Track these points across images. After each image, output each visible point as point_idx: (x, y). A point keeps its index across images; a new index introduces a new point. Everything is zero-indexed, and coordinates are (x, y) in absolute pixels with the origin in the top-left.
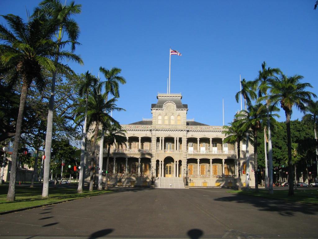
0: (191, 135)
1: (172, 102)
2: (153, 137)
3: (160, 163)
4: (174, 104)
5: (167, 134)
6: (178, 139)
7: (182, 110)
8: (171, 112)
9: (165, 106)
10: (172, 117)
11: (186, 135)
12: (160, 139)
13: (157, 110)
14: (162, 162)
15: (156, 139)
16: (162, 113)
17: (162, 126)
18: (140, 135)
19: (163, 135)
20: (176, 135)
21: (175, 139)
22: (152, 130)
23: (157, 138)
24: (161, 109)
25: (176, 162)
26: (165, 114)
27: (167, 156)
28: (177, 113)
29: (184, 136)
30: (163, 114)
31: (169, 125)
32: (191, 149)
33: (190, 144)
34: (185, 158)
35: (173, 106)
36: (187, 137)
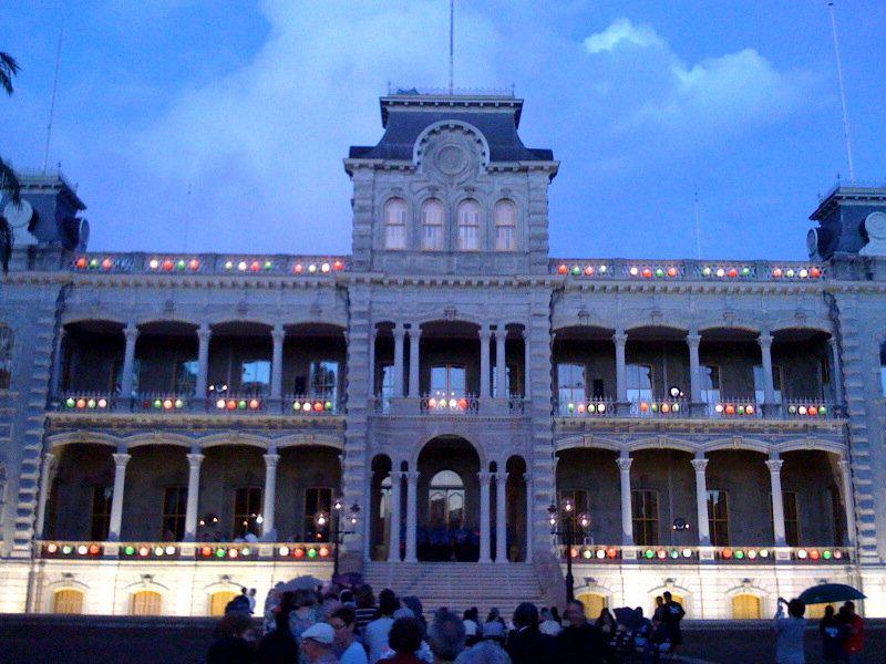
0: (576, 312)
1: (467, 126)
2: (355, 322)
3: (396, 472)
4: (479, 135)
5: (438, 305)
6: (502, 333)
7: (525, 170)
8: (456, 180)
9: (429, 148)
10: (468, 213)
11: (547, 311)
12: (399, 331)
13: (377, 168)
15: (375, 331)
16: (410, 186)
18: (279, 313)
19: (413, 310)
20: (487, 311)
21: (485, 333)
22: (348, 282)
23: (377, 325)
24: (402, 164)
25: (493, 467)
26: (425, 193)
27: (435, 434)
28: (498, 188)
29: (535, 315)
30: (415, 194)
31: (451, 253)
32: (576, 404)
33: (573, 373)
34: (544, 442)
35: (473, 152)
36: (555, 328)
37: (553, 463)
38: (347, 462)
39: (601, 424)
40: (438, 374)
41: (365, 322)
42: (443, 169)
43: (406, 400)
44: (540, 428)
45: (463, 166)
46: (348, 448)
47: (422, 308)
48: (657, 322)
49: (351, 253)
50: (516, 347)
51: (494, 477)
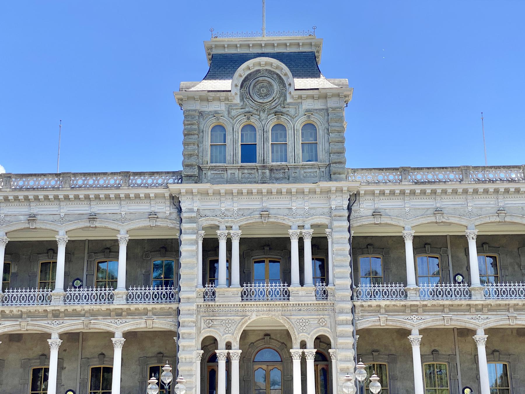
0: (370, 212)
14: (229, 346)
17: (229, 172)
25: (303, 345)
27: (254, 318)
31: (264, 167)
37: (351, 341)
38: (182, 343)
39: (394, 305)
40: (258, 269)
41: (194, 225)
42: (256, 98)
43: (229, 289)
44: (341, 312)
45: (274, 96)
46: (182, 331)
47: (241, 213)
48: (439, 218)
49: (181, 169)
50: (320, 246)
51: (303, 353)
